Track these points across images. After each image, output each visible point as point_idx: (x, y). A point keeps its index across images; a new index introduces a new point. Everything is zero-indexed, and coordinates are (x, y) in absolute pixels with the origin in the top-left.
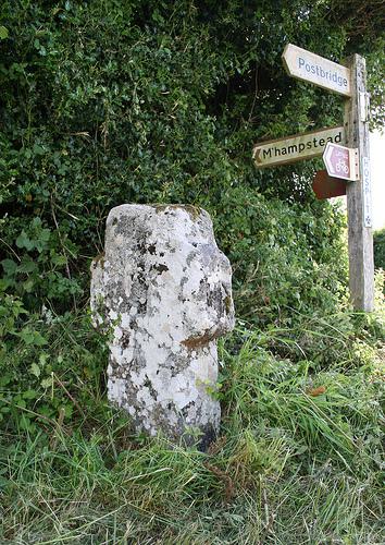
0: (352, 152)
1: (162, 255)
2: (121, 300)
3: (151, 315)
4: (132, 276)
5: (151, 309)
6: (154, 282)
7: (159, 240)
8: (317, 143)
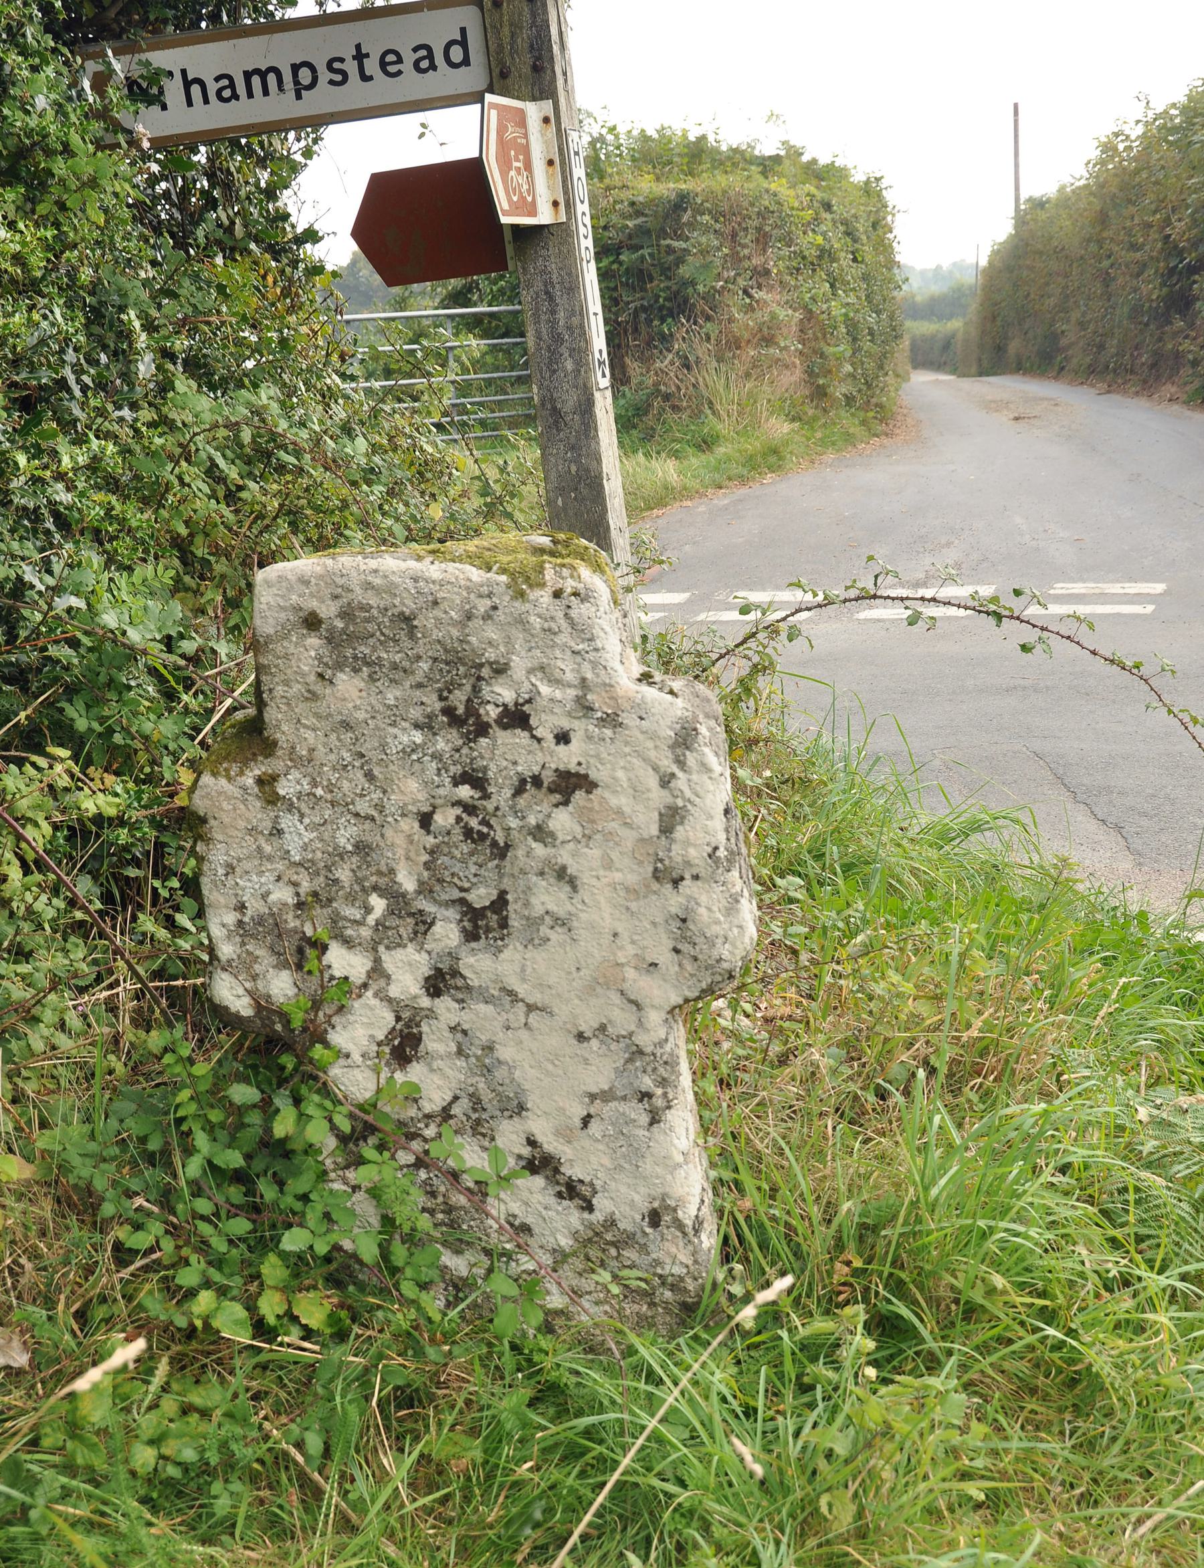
0: (534, 111)
1: (563, 738)
2: (378, 904)
3: (533, 941)
4: (425, 820)
5: (533, 923)
6: (540, 833)
7: (545, 689)
8: (372, 66)
